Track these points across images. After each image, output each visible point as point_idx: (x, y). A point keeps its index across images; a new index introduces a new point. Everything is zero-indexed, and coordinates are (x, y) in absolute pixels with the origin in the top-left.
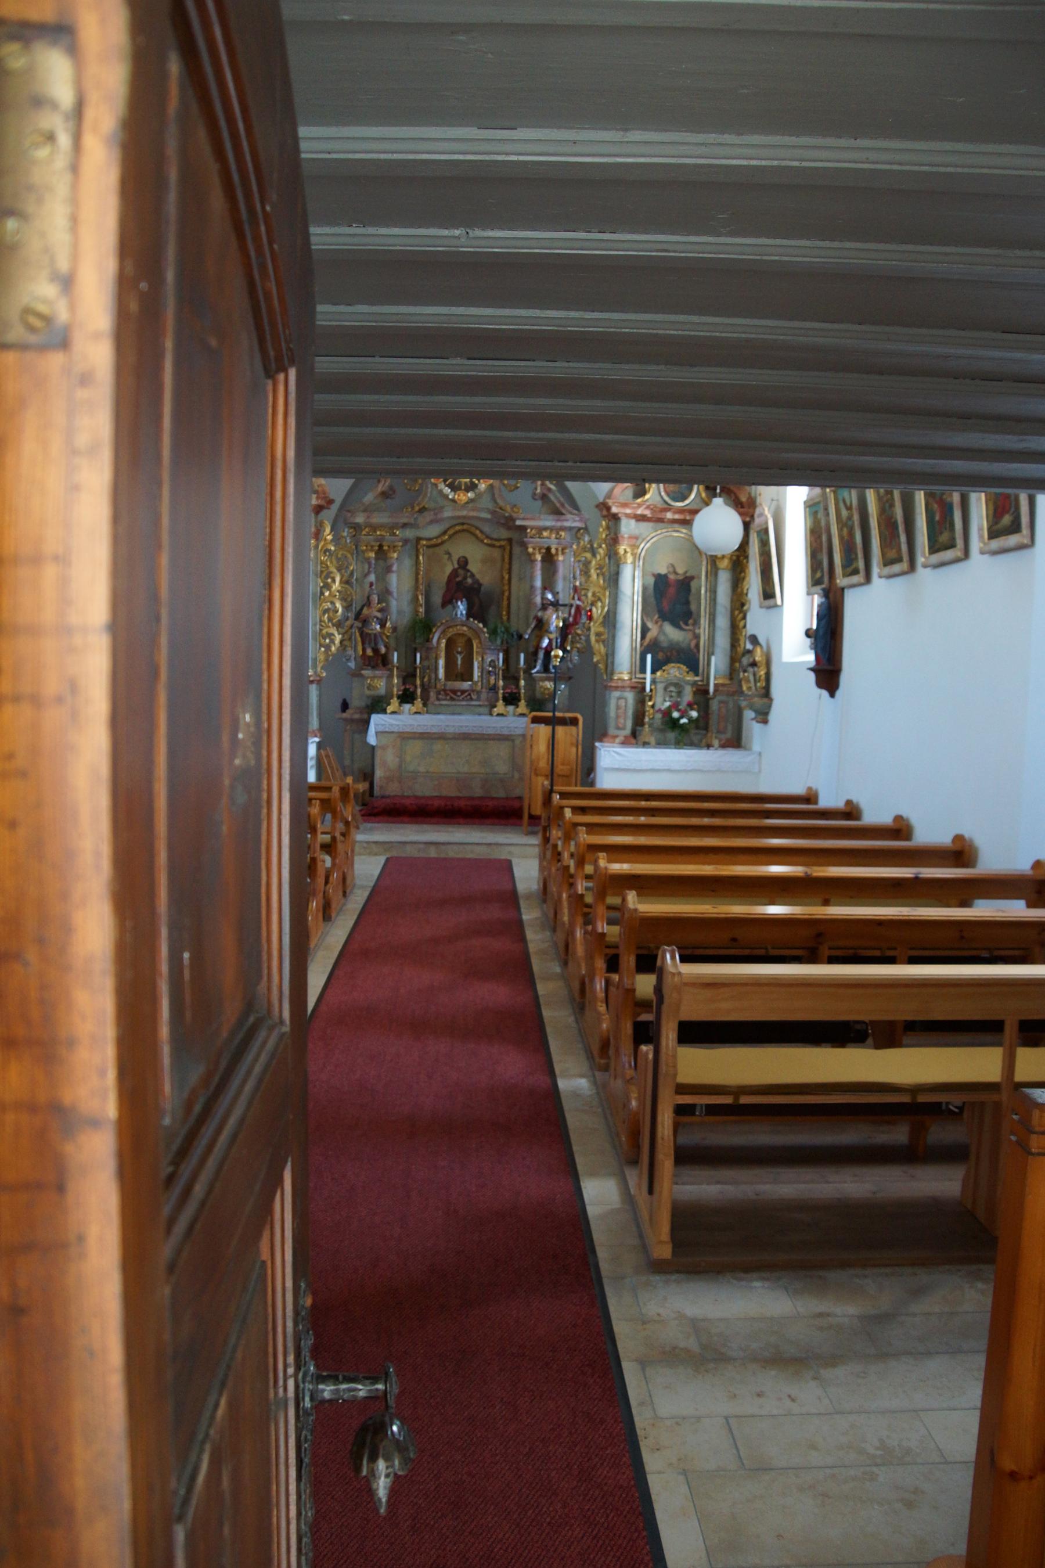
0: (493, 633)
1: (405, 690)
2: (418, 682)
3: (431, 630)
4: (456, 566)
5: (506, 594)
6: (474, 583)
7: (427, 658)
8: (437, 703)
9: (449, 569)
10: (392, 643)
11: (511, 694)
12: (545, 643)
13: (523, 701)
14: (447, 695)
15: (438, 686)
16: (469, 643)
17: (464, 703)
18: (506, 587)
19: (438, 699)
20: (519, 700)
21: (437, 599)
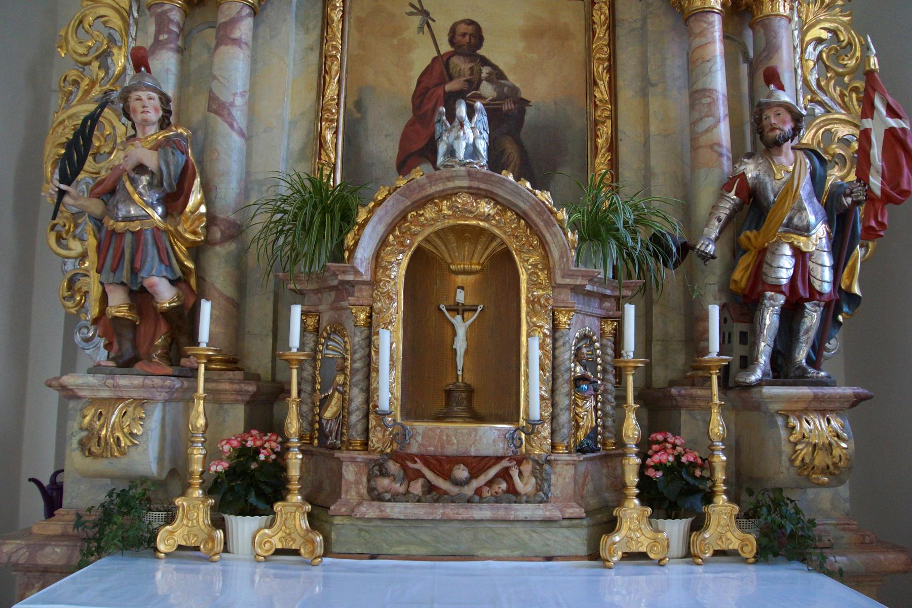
0: (595, 230)
1: (245, 454)
2: (293, 425)
3: (347, 218)
4: (445, 48)
5: (605, 130)
6: (501, 97)
7: (338, 329)
8: (370, 510)
9: (422, 57)
10: (219, 274)
11: (676, 470)
12: (784, 267)
13: (721, 499)
14: (410, 475)
15: (376, 440)
16: (502, 265)
17: (484, 512)
18: (603, 112)
19: (375, 496)
20: (709, 498)
21: (384, 145)
